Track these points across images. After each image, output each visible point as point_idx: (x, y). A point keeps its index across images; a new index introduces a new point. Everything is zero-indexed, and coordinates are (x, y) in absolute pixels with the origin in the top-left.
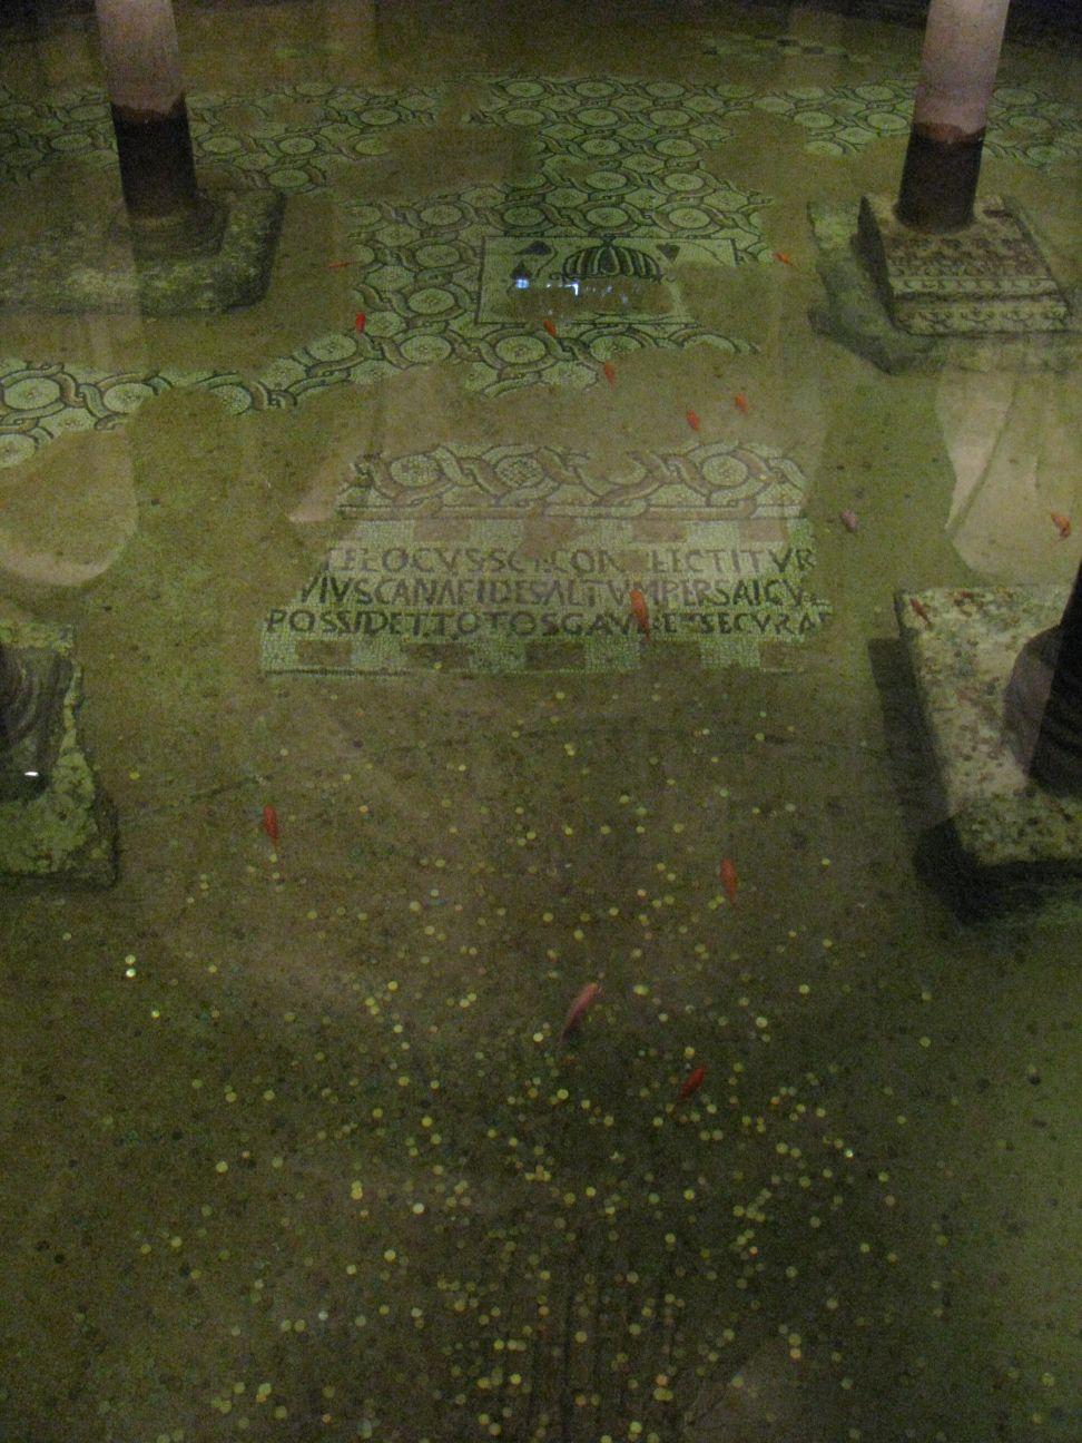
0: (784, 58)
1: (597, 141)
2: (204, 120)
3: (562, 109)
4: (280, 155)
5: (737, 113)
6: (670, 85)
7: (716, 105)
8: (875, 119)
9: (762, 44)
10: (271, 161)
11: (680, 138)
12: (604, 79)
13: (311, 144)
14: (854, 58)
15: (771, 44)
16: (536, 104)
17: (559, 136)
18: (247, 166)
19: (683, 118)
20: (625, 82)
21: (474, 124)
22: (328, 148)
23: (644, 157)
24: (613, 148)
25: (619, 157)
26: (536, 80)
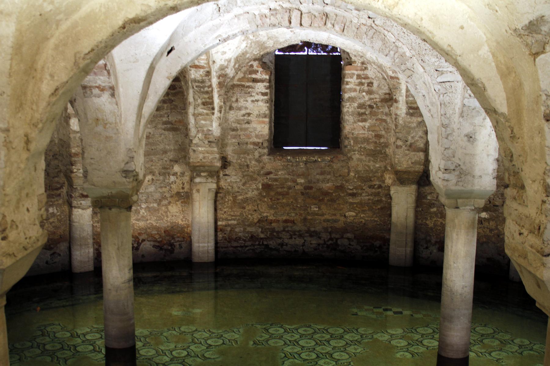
0: (386, 316)
1: (307, 353)
2: (141, 341)
3: (292, 339)
4: (172, 357)
5: (367, 340)
6: (338, 329)
7: (358, 337)
8: (425, 342)
9: (375, 310)
10: (168, 359)
11: (342, 352)
12: (309, 326)
13: (185, 353)
14: (416, 316)
15: (381, 310)
16: (281, 337)
17: (290, 351)
18: (158, 361)
19: (342, 343)
20: (319, 327)
21: (254, 346)
22: (193, 354)
23: (327, 360)
24: (314, 356)
25: (316, 360)
26: (281, 327)
